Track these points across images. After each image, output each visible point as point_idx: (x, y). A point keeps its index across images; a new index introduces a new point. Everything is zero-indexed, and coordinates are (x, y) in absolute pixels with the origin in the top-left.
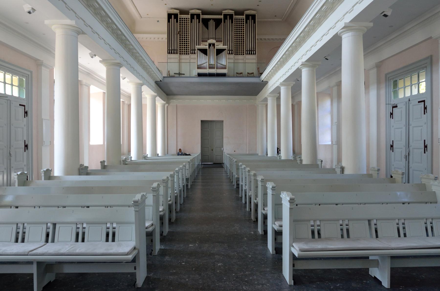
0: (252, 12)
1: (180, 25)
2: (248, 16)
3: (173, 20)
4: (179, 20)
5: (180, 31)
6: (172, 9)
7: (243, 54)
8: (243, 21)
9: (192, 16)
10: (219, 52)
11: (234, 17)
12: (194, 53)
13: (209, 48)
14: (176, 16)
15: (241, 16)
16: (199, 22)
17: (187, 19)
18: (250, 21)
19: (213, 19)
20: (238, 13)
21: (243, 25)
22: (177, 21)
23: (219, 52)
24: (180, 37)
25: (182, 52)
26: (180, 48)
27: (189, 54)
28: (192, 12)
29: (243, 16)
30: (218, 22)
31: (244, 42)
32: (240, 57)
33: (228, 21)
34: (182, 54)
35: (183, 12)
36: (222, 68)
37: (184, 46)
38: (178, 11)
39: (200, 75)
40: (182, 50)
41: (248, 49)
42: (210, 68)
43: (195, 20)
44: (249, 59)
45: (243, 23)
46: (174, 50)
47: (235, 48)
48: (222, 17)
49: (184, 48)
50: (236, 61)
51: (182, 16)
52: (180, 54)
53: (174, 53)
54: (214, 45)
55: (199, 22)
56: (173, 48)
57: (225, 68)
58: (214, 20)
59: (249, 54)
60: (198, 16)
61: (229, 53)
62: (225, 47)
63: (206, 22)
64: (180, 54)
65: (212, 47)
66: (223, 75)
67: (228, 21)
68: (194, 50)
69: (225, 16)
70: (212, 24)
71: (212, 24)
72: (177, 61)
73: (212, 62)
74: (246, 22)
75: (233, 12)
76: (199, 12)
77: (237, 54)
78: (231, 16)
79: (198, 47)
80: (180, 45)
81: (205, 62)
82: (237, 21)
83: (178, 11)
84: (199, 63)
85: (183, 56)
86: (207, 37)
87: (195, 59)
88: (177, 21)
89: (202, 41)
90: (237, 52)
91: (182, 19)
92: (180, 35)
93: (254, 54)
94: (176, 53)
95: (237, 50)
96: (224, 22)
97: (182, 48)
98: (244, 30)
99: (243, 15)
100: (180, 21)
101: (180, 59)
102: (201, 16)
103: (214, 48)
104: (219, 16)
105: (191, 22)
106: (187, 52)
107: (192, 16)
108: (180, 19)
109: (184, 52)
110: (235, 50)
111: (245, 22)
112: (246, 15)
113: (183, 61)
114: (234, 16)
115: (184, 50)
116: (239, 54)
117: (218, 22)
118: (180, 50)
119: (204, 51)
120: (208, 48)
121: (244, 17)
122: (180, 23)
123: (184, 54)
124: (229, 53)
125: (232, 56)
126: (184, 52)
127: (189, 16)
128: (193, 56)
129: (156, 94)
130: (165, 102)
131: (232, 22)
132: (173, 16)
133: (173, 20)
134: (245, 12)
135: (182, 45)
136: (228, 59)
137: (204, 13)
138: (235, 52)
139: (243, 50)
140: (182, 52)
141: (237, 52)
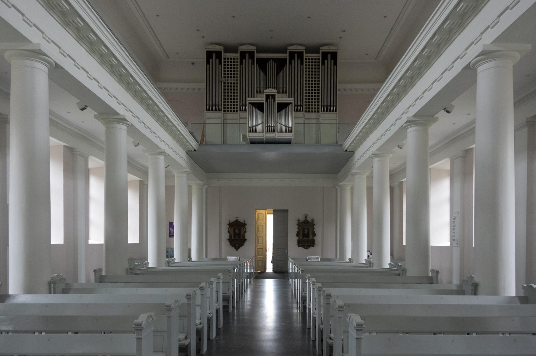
0: (332, 49)
1: (225, 68)
2: (325, 55)
5: (225, 77)
8: (319, 62)
10: (282, 107)
11: (305, 56)
12: (245, 110)
14: (218, 54)
16: (253, 63)
17: (234, 59)
18: (329, 62)
20: (310, 50)
21: (319, 68)
24: (224, 86)
25: (228, 108)
26: (225, 102)
27: (237, 111)
29: (318, 55)
30: (281, 64)
31: (318, 93)
32: (313, 115)
33: (296, 62)
34: (228, 111)
35: (230, 49)
36: (286, 131)
38: (222, 47)
39: (253, 142)
41: (325, 104)
42: (267, 131)
45: (319, 65)
46: (216, 105)
47: (306, 102)
48: (287, 56)
49: (231, 102)
50: (307, 122)
51: (228, 54)
52: (225, 111)
53: (216, 110)
54: (273, 96)
55: (253, 63)
58: (275, 60)
59: (327, 111)
60: (251, 54)
61: (297, 110)
62: (291, 100)
63: (263, 64)
64: (225, 111)
65: (271, 100)
66: (288, 142)
67: (296, 62)
68: (246, 105)
69: (292, 54)
70: (271, 67)
71: (271, 67)
72: (220, 121)
73: (271, 123)
74: (323, 64)
75: (303, 48)
76: (252, 48)
77: (309, 112)
78: (300, 55)
79: (250, 100)
80: (225, 99)
81: (260, 122)
83: (222, 47)
84: (252, 124)
85: (229, 115)
87: (246, 118)
88: (220, 63)
89: (257, 92)
90: (309, 108)
91: (228, 59)
92: (225, 83)
94: (219, 110)
95: (309, 105)
97: (228, 102)
98: (319, 75)
99: (318, 53)
100: (225, 62)
102: (256, 54)
105: (241, 63)
106: (234, 108)
107: (243, 55)
108: (225, 59)
109: (231, 108)
110: (306, 105)
114: (305, 55)
115: (231, 105)
116: (312, 112)
117: (281, 64)
118: (225, 105)
119: (259, 107)
121: (320, 56)
122: (225, 65)
123: (231, 111)
124: (297, 110)
125: (300, 114)
126: (231, 108)
127: (239, 55)
128: (243, 114)
130: (203, 183)
131: (302, 64)
132: (214, 55)
134: (322, 48)
135: (228, 99)
136: (295, 118)
137: (260, 50)
138: (306, 108)
139: (318, 105)
140: (228, 108)
141: (309, 108)
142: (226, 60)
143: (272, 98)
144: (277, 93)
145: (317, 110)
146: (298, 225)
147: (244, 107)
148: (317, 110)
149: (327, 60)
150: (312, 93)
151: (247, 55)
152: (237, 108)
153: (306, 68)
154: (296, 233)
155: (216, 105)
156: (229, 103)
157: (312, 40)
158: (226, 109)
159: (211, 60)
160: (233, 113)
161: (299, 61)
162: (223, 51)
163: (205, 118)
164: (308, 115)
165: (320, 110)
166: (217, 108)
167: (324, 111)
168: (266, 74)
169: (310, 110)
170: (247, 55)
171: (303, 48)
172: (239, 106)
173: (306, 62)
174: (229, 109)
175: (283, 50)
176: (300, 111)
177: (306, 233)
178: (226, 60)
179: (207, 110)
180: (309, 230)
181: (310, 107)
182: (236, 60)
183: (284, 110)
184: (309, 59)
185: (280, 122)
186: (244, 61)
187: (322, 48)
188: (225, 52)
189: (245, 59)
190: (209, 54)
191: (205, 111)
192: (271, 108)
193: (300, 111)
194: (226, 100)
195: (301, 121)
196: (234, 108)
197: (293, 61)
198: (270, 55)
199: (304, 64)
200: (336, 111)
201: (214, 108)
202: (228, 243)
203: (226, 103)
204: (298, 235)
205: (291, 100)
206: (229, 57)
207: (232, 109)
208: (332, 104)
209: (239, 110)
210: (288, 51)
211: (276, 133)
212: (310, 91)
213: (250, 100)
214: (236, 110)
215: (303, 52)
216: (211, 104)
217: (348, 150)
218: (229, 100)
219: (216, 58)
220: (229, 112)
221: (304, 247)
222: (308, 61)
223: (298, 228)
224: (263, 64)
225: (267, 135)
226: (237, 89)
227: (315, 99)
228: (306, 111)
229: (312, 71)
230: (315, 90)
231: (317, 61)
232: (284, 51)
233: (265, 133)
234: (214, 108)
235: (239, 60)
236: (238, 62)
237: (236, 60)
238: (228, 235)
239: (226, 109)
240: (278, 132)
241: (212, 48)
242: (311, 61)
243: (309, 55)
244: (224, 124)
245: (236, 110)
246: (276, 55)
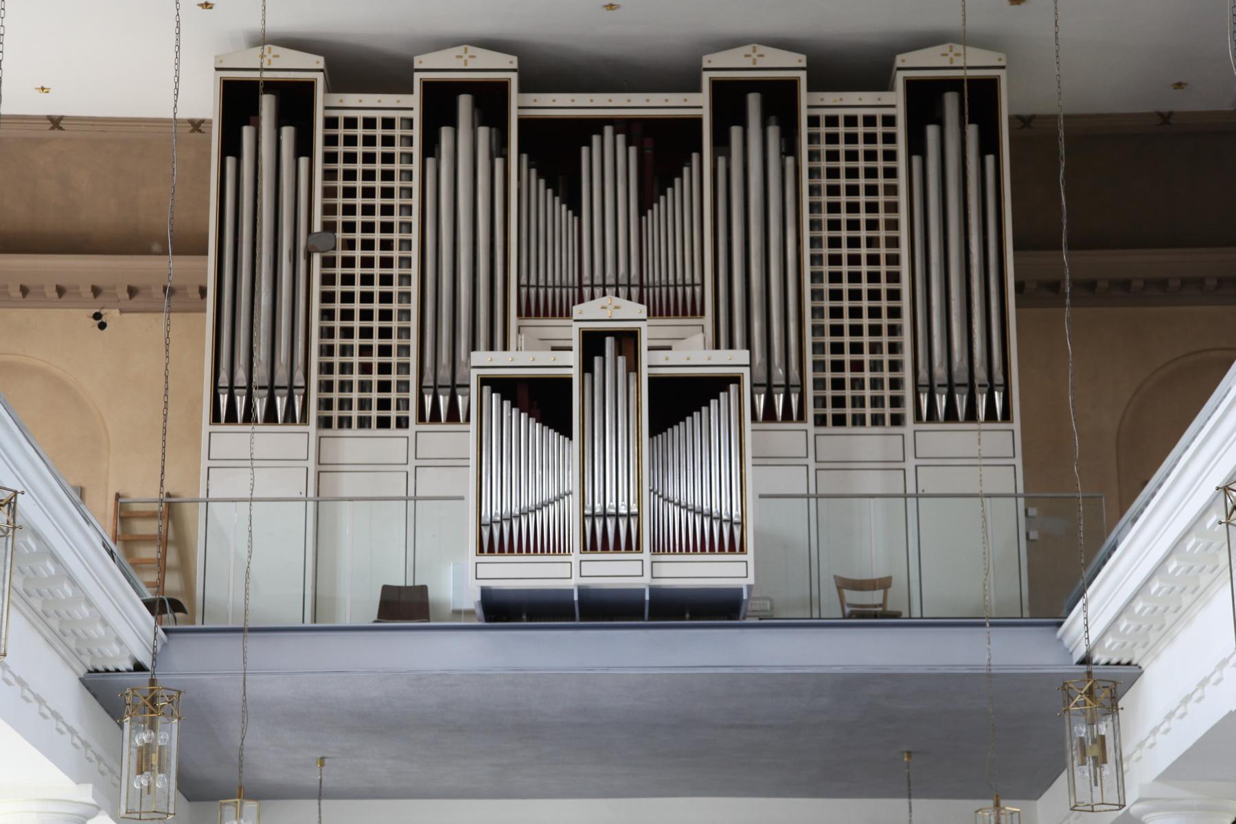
0: (973, 61)
1: (329, 175)
2: (925, 99)
3: (266, 132)
5: (329, 227)
6: (262, 40)
7: (897, 420)
8: (890, 138)
9: (440, 101)
10: (677, 400)
13: (587, 367)
14: (294, 101)
15: (869, 97)
16: (499, 148)
17: (388, 123)
18: (952, 134)
20: (838, 68)
21: (891, 173)
22: (304, 147)
23: (677, 400)
24: (328, 280)
25: (345, 404)
26: (327, 368)
27: (402, 423)
28: (438, 64)
29: (885, 97)
30: (663, 152)
32: (868, 443)
33: (755, 136)
34: (345, 422)
35: (355, 68)
37: (366, 350)
38: (318, 61)
39: (501, 610)
40: (345, 386)
41: (940, 372)
42: (591, 545)
43: (465, 136)
44: (943, 462)
45: (890, 156)
46: (272, 389)
48: (699, 104)
49: (366, 369)
50: (829, 483)
51: (352, 99)
52: (325, 423)
54: (627, 341)
56: (261, 374)
57: (735, 546)
58: (630, 128)
59: (951, 416)
60: (490, 100)
61: (770, 415)
62: (733, 360)
63: (556, 154)
64: (325, 423)
65: (611, 360)
66: (719, 608)
67: (755, 136)
68: (454, 389)
69: (729, 98)
70: (609, 167)
71: (609, 167)
72: (294, 482)
73: (616, 494)
74: (917, 146)
75: (799, 60)
76: (500, 66)
77: (839, 421)
78: (779, 99)
79: (487, 360)
80: (328, 350)
81: (551, 493)
82: (832, 138)
83: (318, 61)
84: (494, 508)
85: (354, 446)
86: (571, 277)
87: (457, 463)
88: (304, 147)
89: (526, 311)
90: (839, 402)
91: (351, 123)
92: (328, 262)
93: (991, 416)
94: (290, 418)
95: (838, 384)
96: (721, 142)
99: (885, 85)
100: (330, 140)
101: (323, 468)
103: (633, 366)
104: (676, 99)
105: (430, 147)
106: (384, 404)
107: (440, 101)
108: (331, 123)
109: (364, 404)
110: (819, 384)
111: (901, 147)
112: (913, 87)
113: (348, 484)
114: (805, 97)
115: (365, 386)
116: (859, 420)
117: (663, 152)
119: (545, 401)
120: (575, 373)
121: (895, 100)
122: (330, 158)
123: (364, 423)
124: (770, 415)
125: (790, 438)
127: (413, 102)
128: (440, 440)
129: (85, 794)
131: (790, 147)
132: (267, 103)
133: (266, 132)
134: (900, 60)
136: (762, 460)
137: (542, 72)
138: (820, 402)
139: (896, 384)
140: (345, 404)
141: (839, 402)
142: (341, 132)
143: (619, 351)
144: (652, 313)
145: (887, 411)
147: (443, 401)
148: (887, 411)
149: (941, 123)
150: (856, 330)
151: (465, 103)
152: (403, 404)
153: (813, 173)
155: (272, 389)
156: (356, 377)
158: (335, 413)
159: (247, 132)
160: (375, 431)
161: (773, 132)
162: (320, 79)
163: (205, 463)
164: (837, 442)
165: (908, 410)
166: (281, 403)
167: (932, 417)
168: (574, 205)
169: (849, 411)
170: (465, 103)
171: (799, 60)
172: (412, 395)
173: (813, 138)
174: (355, 413)
176: (787, 416)
178: (341, 132)
179: (216, 419)
181: (848, 393)
182: (397, 132)
183: (692, 423)
184: (832, 121)
185: (671, 492)
186: (446, 133)
187: (900, 60)
188: (332, 88)
189: (453, 123)
190: (239, 99)
191: (206, 425)
192: (618, 408)
193: (787, 416)
194: (337, 359)
195: (794, 480)
196: (384, 404)
197: (736, 132)
199: (804, 147)
200: (1007, 416)
201: (260, 407)
203: (336, 395)
205: (733, 360)
206: (360, 115)
207: (374, 413)
208: (981, 374)
209: (412, 413)
210: (706, 77)
211: (646, 555)
212: (845, 286)
213: (485, 361)
214: (393, 414)
215: (791, 86)
216: (241, 377)
217: (1098, 657)
218: (356, 359)
219: (281, 120)
220: (355, 431)
222: (823, 130)
225: (588, 569)
226: (405, 314)
227: (875, 348)
228: (820, 421)
229: (852, 191)
230: (874, 277)
231: (879, 130)
233: (576, 556)
234: (260, 407)
235: (416, 133)
236: (409, 141)
237: (397, 132)
239: (335, 413)
240: (656, 549)
241: (252, 64)
242: (842, 130)
243: (830, 98)
244: (320, 498)
245: (393, 414)
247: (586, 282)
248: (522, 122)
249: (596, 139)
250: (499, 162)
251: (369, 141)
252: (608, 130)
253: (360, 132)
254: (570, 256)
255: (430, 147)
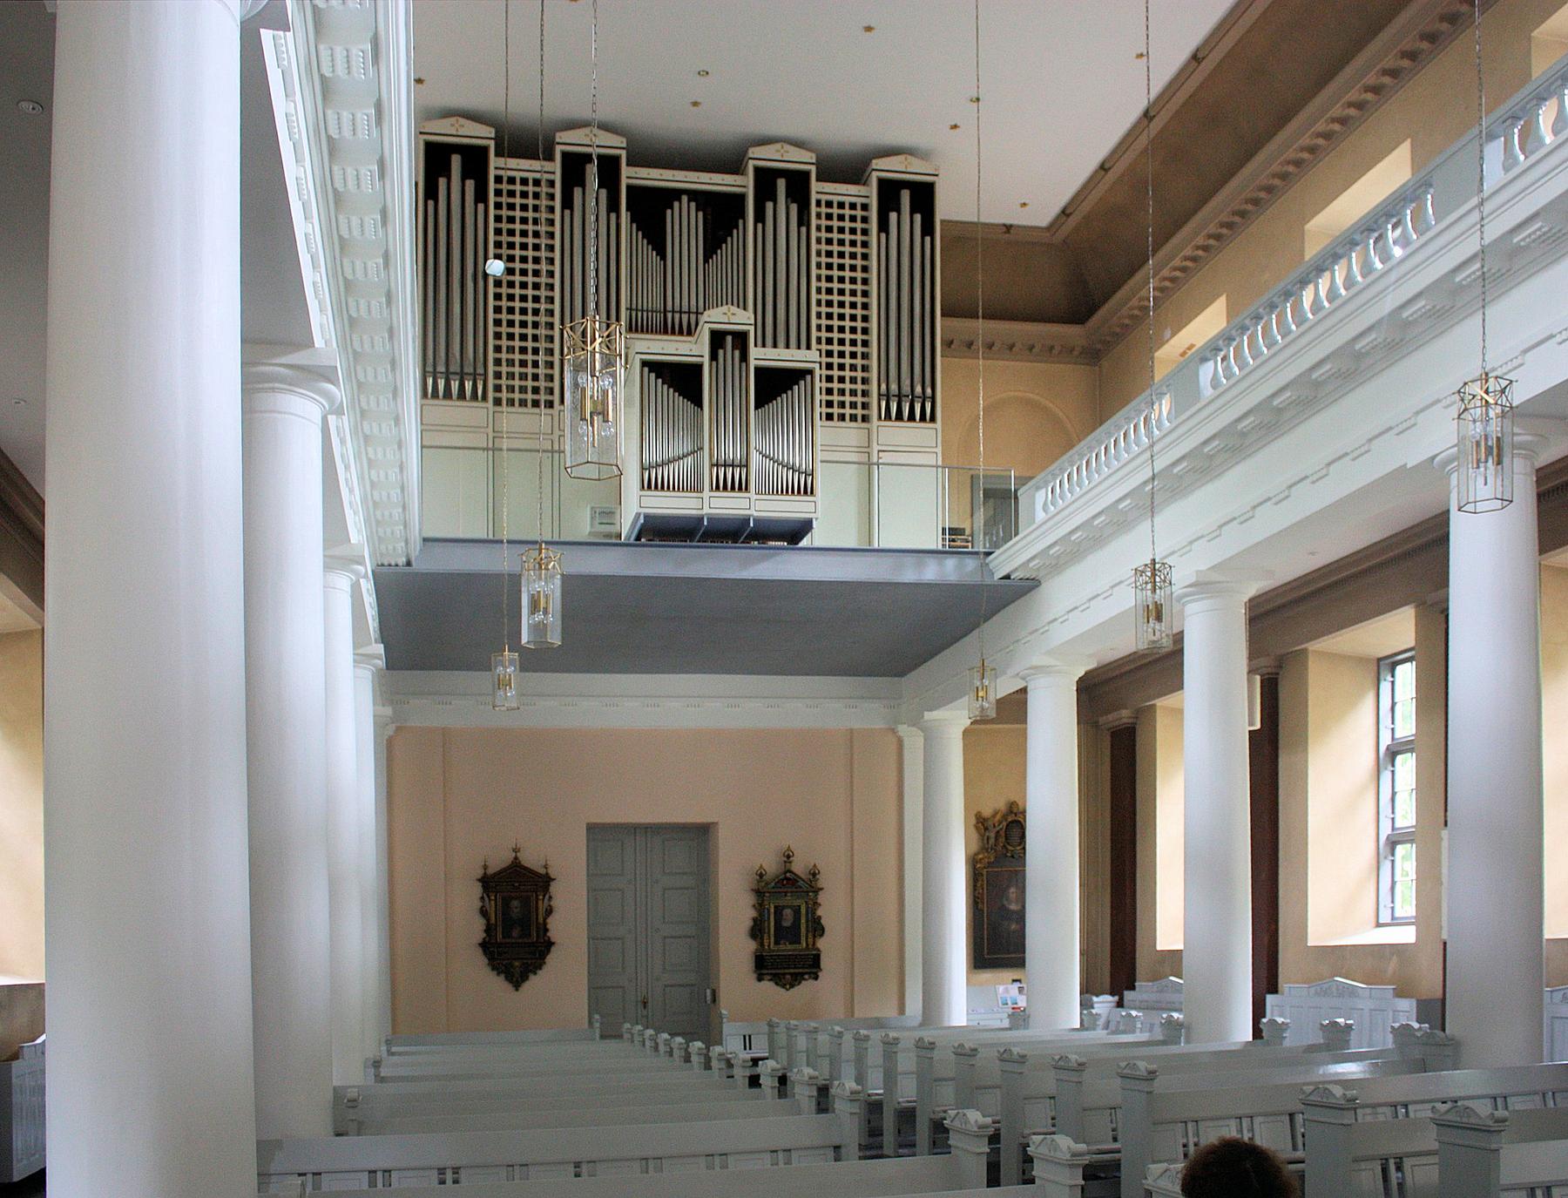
4: (492, 186)
11: (815, 186)
16: (613, 206)
19: (694, 195)
22: (481, 196)
28: (571, 140)
48: (744, 184)
55: (613, 206)
63: (650, 210)
69: (766, 179)
70: (685, 224)
71: (685, 224)
112: (882, 183)
137: (642, 156)
146: (759, 893)
154: (749, 923)
157: (845, 124)
166: (468, 385)
175: (732, 163)
177: (786, 924)
180: (797, 911)
198: (680, 175)
201: (455, 386)
202: (480, 959)
204: (757, 931)
221: (778, 980)
223: (760, 907)
224: (650, 210)
232: (732, 163)
234: (455, 386)
238: (479, 924)
246: (705, 177)
247: (669, 307)
248: (629, 187)
249: (676, 204)
250: (613, 216)
251: (524, 195)
252: (685, 198)
253: (518, 188)
254: (658, 290)
255: (567, 203)
